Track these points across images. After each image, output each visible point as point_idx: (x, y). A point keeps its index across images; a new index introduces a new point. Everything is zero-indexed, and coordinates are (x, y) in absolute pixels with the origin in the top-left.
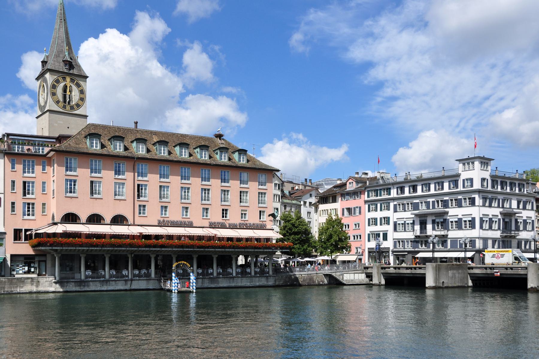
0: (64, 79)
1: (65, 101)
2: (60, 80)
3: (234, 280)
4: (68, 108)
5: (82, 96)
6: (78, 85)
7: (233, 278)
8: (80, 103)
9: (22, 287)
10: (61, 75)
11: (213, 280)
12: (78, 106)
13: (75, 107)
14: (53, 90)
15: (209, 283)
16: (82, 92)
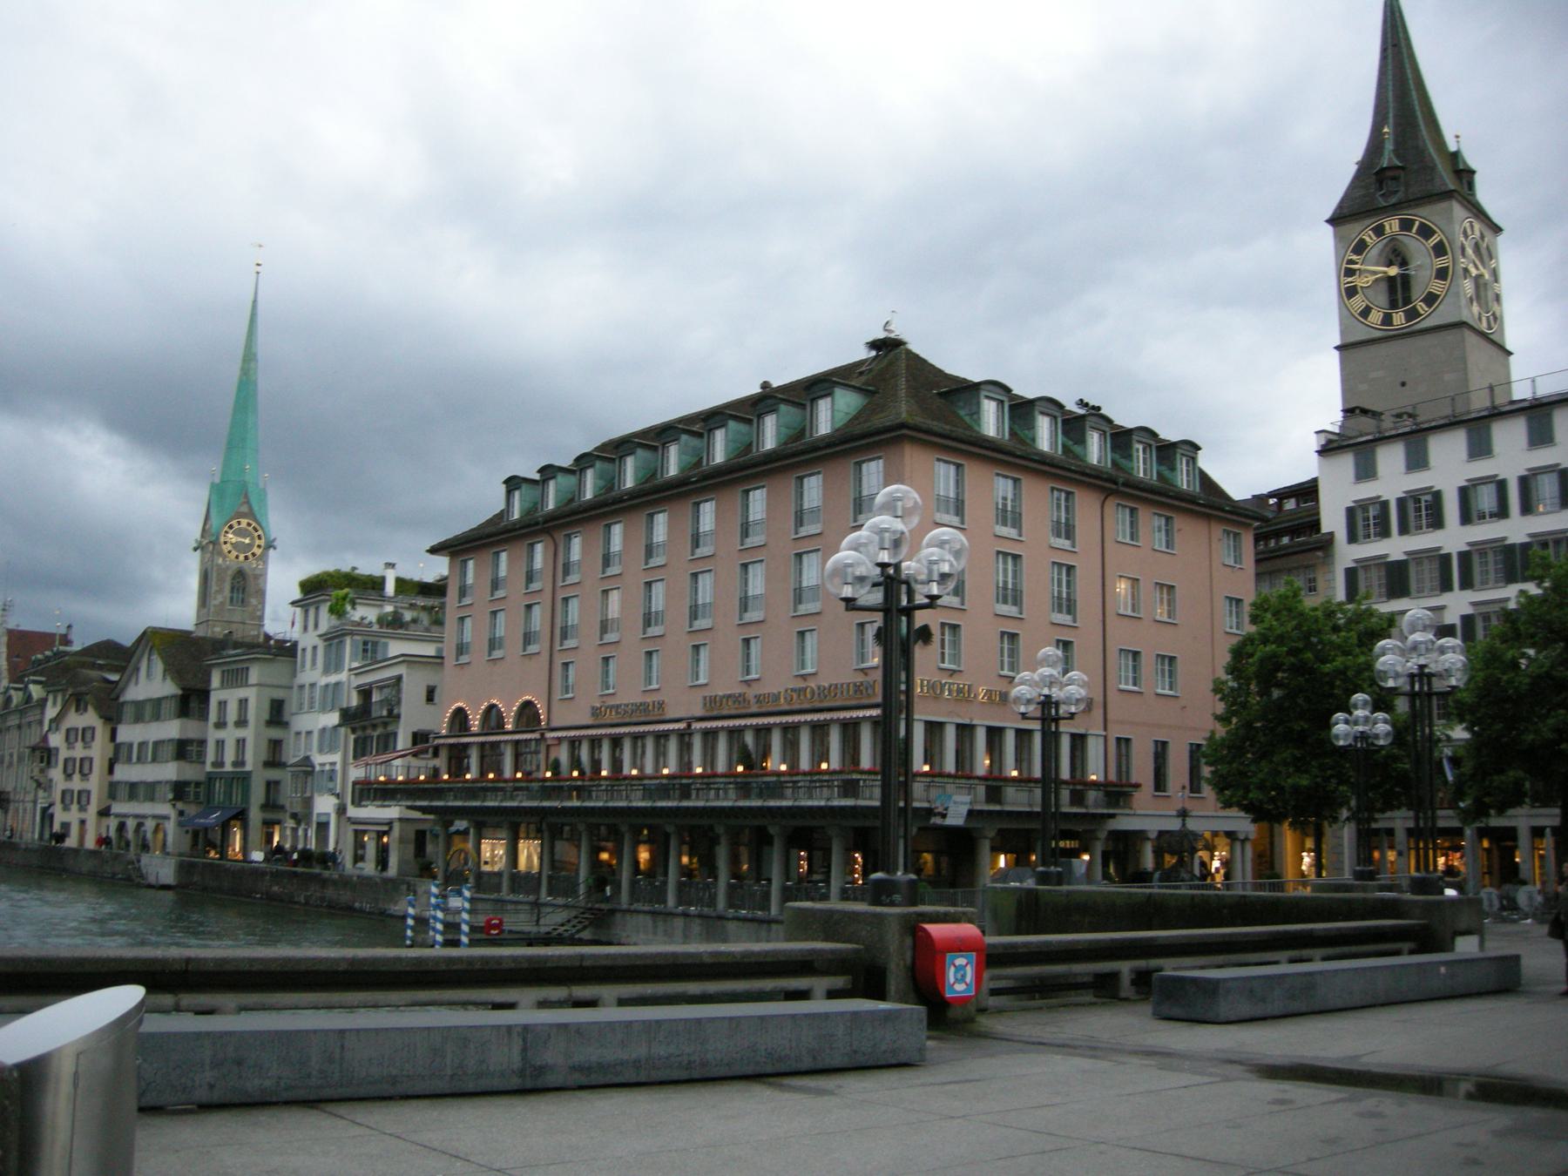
0: (1379, 231)
1: (1393, 305)
2: (1368, 239)
3: (769, 931)
4: (1399, 318)
5: (1440, 263)
6: (1426, 232)
7: (770, 922)
8: (1437, 287)
9: (396, 903)
10: (1368, 222)
11: (713, 925)
12: (1431, 299)
13: (1421, 307)
14: (1350, 279)
15: (700, 935)
16: (1440, 250)
